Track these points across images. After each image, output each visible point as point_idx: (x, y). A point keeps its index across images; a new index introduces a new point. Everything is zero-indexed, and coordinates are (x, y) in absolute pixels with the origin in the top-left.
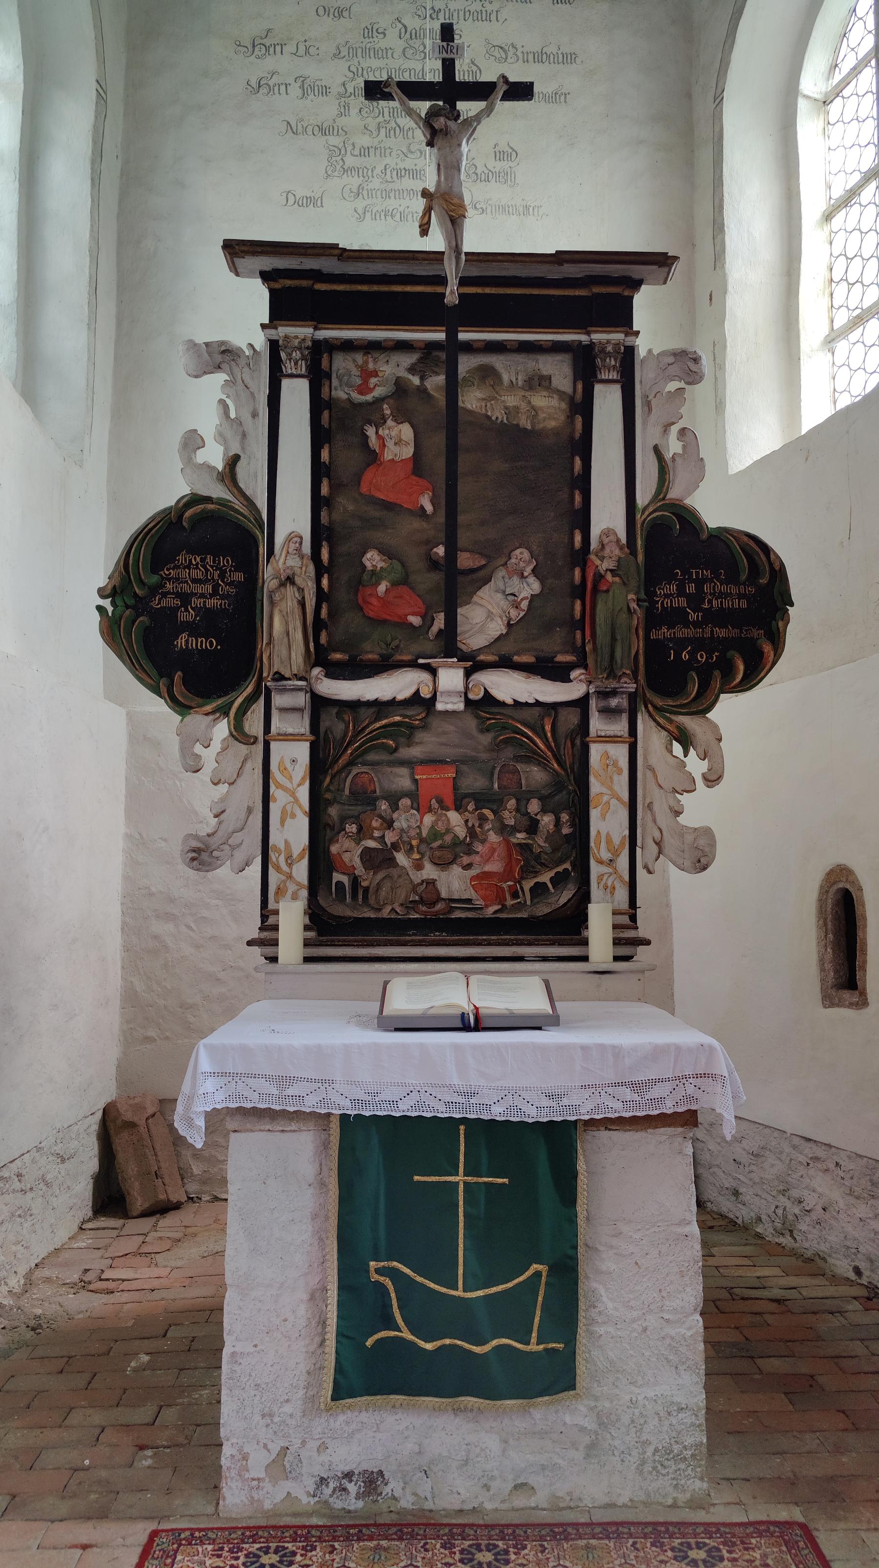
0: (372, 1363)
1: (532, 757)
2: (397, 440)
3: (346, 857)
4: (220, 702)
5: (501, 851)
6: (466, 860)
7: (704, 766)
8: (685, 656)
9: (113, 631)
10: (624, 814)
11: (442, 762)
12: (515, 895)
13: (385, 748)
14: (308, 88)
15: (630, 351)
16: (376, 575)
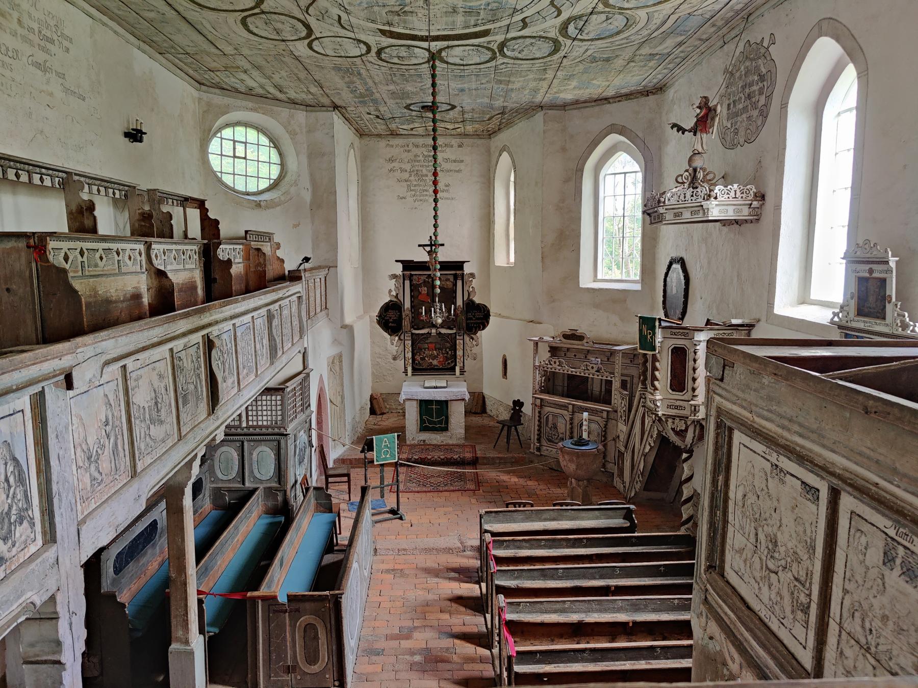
0: (423, 428)
1: (448, 342)
9: (379, 323)
14: (402, 170)
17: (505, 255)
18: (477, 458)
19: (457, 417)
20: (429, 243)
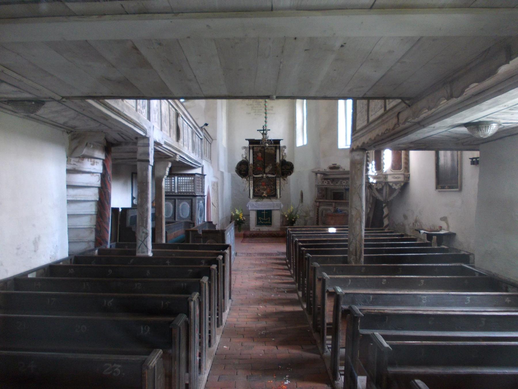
2: (260, 155)
9: (236, 171)
15: (280, 147)
17: (301, 140)
19: (276, 218)
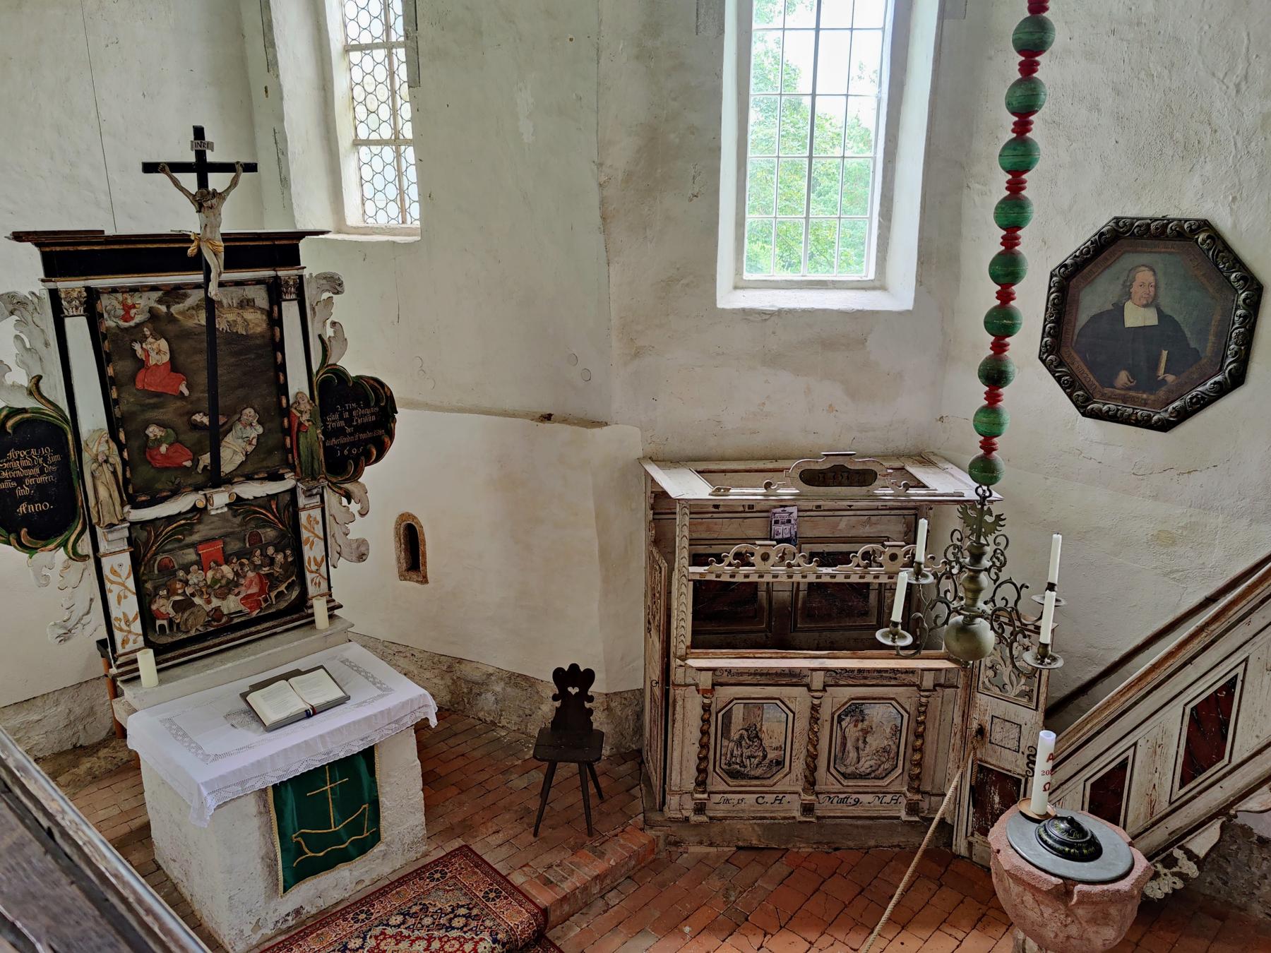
1: (266, 523)
2: (157, 351)
3: (163, 610)
4: (59, 540)
5: (257, 580)
6: (236, 591)
7: (358, 507)
8: (346, 452)
10: (322, 543)
11: (214, 539)
12: (266, 600)
13: (180, 541)
15: (301, 277)
16: (159, 442)
18: (545, 912)
20: (191, 158)
